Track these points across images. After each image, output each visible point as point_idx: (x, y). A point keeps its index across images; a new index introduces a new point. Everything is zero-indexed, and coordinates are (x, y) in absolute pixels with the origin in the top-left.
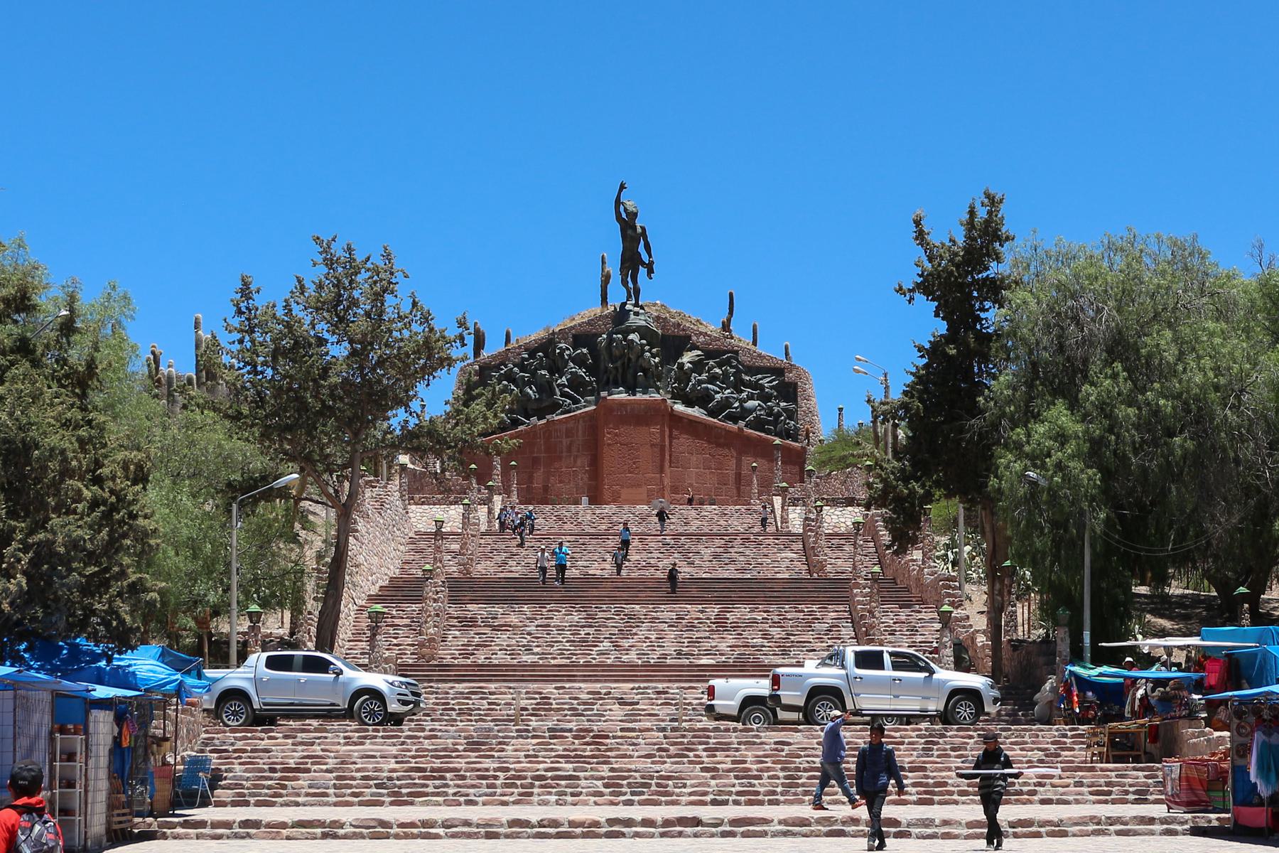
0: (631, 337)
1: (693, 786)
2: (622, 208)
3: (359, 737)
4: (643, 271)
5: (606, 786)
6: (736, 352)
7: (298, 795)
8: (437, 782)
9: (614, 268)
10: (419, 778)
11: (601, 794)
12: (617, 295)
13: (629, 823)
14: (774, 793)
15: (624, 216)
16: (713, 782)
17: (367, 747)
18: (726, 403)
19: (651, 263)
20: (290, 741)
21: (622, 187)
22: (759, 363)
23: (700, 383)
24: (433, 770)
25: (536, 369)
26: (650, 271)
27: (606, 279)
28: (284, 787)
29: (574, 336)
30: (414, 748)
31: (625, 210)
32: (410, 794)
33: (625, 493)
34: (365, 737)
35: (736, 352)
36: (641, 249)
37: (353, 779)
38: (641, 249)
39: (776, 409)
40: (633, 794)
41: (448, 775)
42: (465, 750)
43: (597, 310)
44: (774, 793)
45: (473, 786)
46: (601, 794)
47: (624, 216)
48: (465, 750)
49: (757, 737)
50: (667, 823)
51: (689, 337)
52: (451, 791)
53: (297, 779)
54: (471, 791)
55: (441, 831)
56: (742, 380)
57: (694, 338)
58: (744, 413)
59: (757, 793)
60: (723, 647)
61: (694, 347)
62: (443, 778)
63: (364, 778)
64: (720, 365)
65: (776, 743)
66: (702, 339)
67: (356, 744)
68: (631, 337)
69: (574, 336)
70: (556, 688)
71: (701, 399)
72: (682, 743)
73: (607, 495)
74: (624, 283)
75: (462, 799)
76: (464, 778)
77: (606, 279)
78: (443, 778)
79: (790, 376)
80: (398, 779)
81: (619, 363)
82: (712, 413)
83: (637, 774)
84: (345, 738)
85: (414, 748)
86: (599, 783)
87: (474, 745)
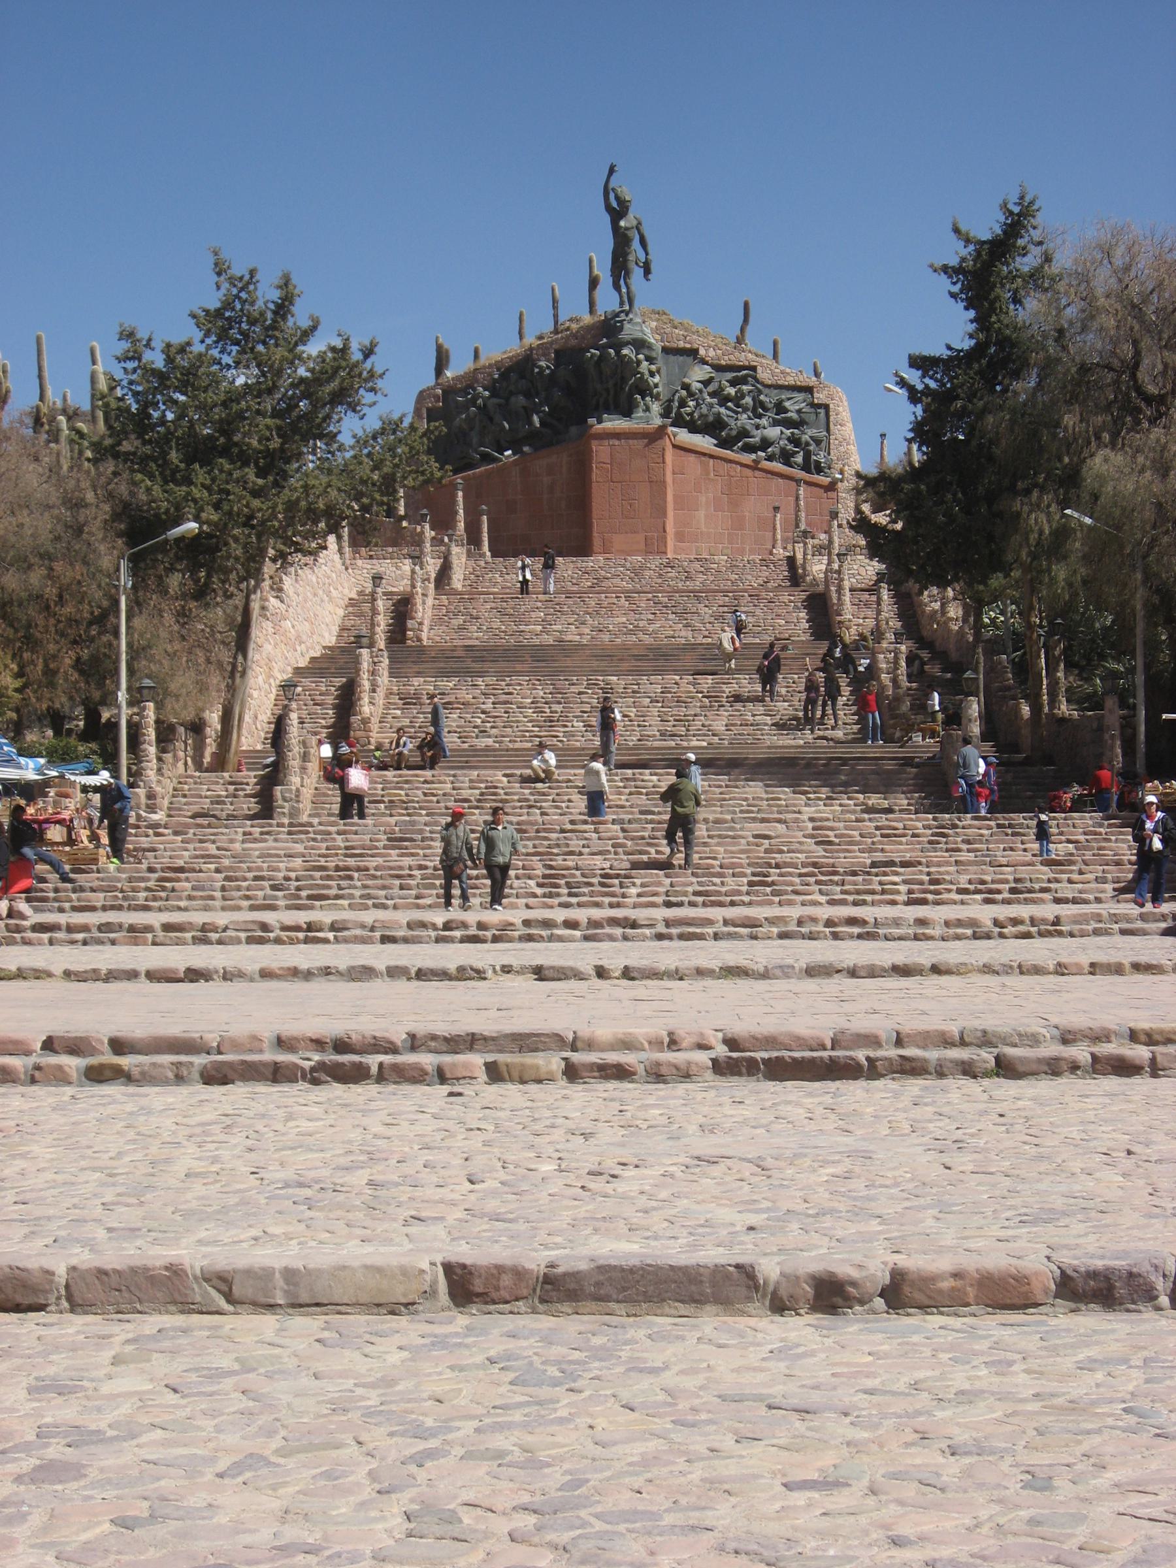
0: (625, 351)
1: (642, 885)
2: (612, 196)
3: (262, 833)
4: (637, 273)
5: (539, 885)
6: (754, 369)
7: (180, 899)
8: (344, 883)
9: (603, 271)
10: (322, 878)
11: (535, 896)
12: (608, 301)
13: (547, 924)
14: (739, 893)
16: (668, 881)
17: (271, 844)
18: (744, 433)
20: (179, 838)
21: (612, 170)
23: (711, 406)
24: (337, 869)
25: (512, 393)
26: (647, 271)
27: (594, 283)
28: (164, 889)
29: (557, 352)
30: (324, 845)
31: (617, 198)
32: (309, 897)
33: (618, 540)
34: (268, 833)
35: (754, 369)
36: (636, 244)
37: (245, 879)
40: (570, 895)
41: (356, 875)
42: (385, 847)
43: (587, 319)
44: (739, 893)
45: (384, 887)
46: (535, 896)
47: (614, 204)
48: (385, 847)
49: (732, 829)
50: (594, 924)
52: (357, 893)
53: (178, 880)
54: (383, 893)
55: (331, 936)
56: (762, 405)
57: (702, 352)
58: (765, 444)
59: (719, 893)
60: (719, 726)
62: (351, 878)
63: (256, 878)
64: (733, 383)
65: (756, 836)
66: (712, 353)
67: (255, 840)
68: (625, 351)
70: (505, 775)
71: (713, 427)
72: (643, 838)
73: (597, 542)
74: (617, 287)
75: (370, 902)
76: (374, 877)
77: (594, 283)
78: (351, 878)
79: (820, 397)
80: (297, 880)
81: (611, 384)
82: (724, 443)
83: (578, 873)
84: (245, 834)
85: (324, 845)
86: (532, 883)
87: (395, 841)
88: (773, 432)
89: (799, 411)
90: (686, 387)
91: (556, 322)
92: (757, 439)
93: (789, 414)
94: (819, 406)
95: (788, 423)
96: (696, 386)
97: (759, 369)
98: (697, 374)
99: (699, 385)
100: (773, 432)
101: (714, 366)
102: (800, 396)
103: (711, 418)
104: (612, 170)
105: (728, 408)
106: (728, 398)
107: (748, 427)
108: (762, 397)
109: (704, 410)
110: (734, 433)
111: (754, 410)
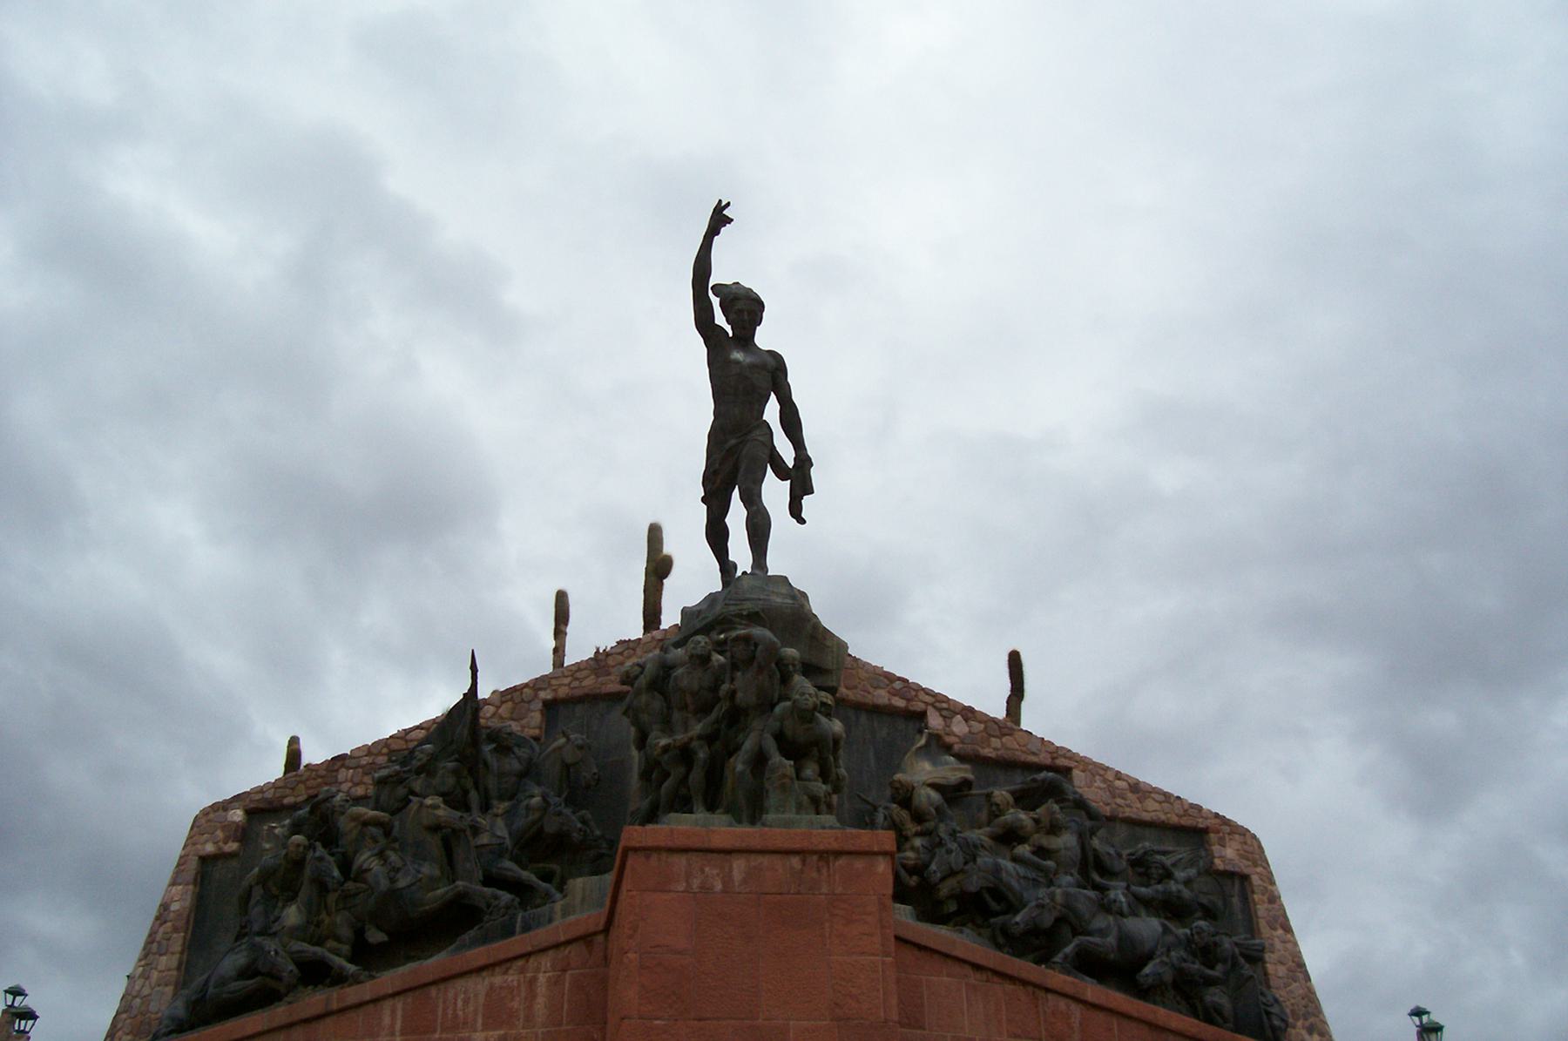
2: (715, 301)
4: (775, 492)
6: (1066, 771)
15: (720, 319)
18: (1069, 922)
19: (803, 461)
21: (719, 219)
22: (1134, 808)
27: (659, 568)
35: (1066, 771)
36: (772, 412)
38: (772, 412)
39: (1227, 943)
43: (635, 630)
47: (720, 319)
51: (922, 715)
57: (935, 721)
61: (939, 746)
64: (1025, 799)
69: (550, 707)
74: (717, 536)
77: (659, 568)
79: (1227, 855)
88: (1147, 927)
89: (1188, 882)
90: (904, 797)
91: (559, 652)
92: (1111, 940)
93: (1173, 886)
94: (1230, 875)
95: (1173, 909)
96: (927, 797)
97: (1076, 772)
98: (922, 772)
99: (935, 795)
100: (1147, 927)
101: (961, 758)
102: (1183, 853)
103: (974, 883)
104: (719, 219)
105: (1015, 859)
106: (1009, 837)
107: (1082, 907)
108: (1096, 843)
109: (956, 859)
110: (1047, 920)
111: (1084, 871)
